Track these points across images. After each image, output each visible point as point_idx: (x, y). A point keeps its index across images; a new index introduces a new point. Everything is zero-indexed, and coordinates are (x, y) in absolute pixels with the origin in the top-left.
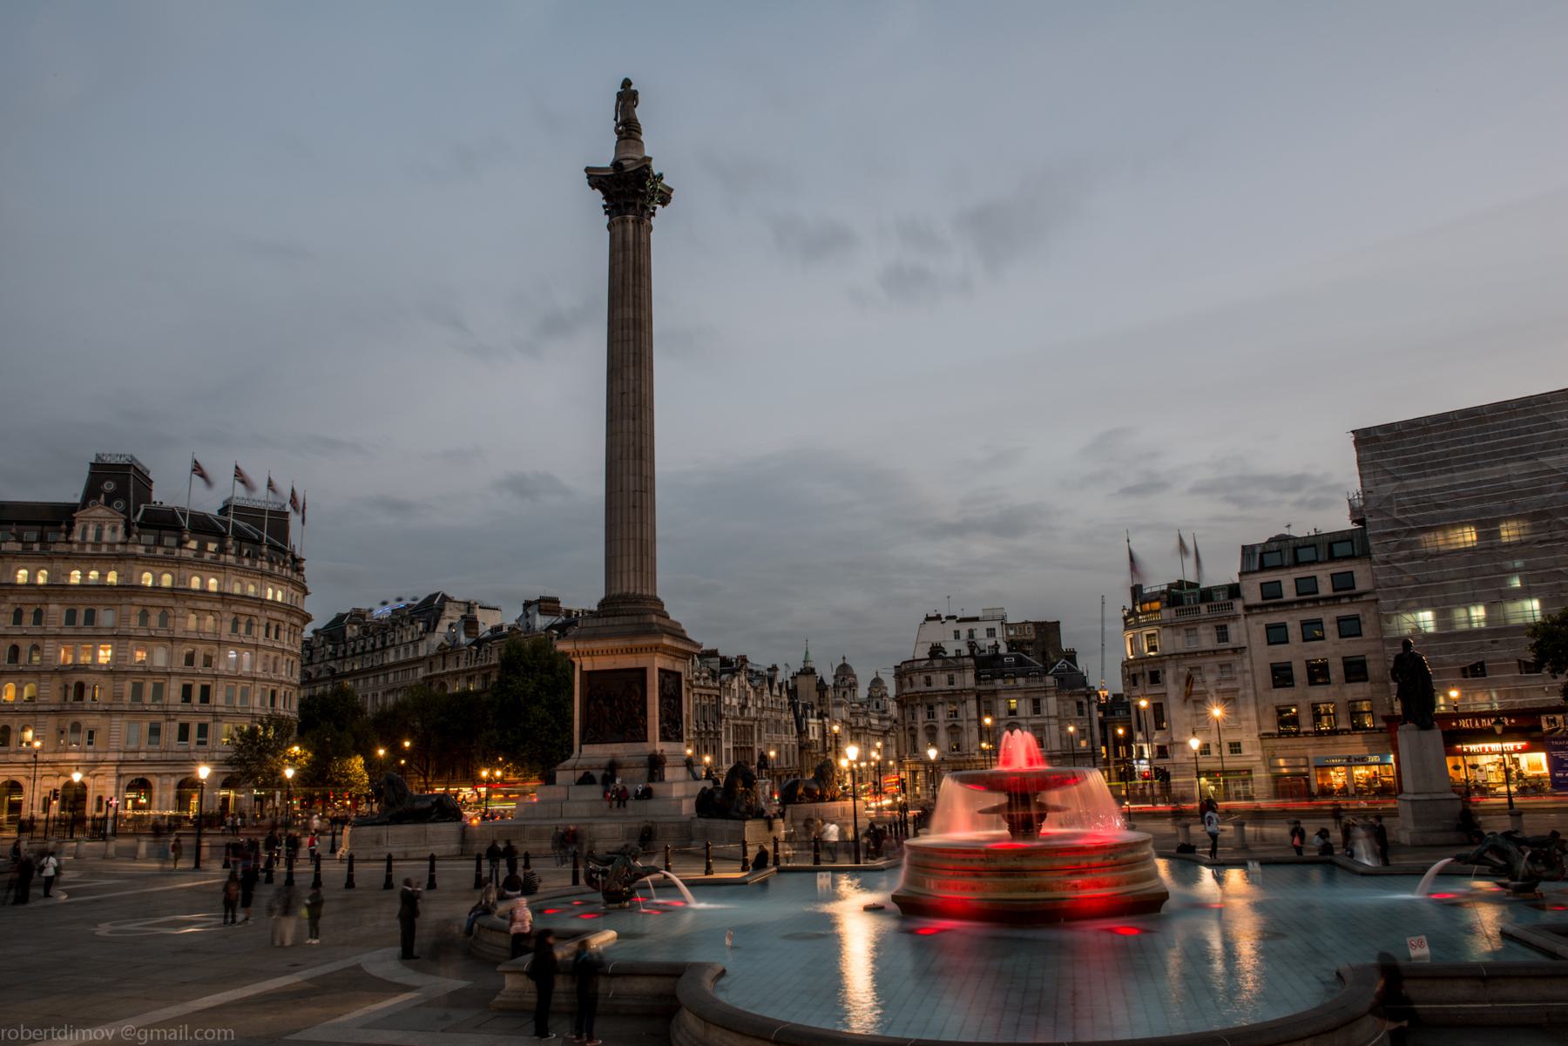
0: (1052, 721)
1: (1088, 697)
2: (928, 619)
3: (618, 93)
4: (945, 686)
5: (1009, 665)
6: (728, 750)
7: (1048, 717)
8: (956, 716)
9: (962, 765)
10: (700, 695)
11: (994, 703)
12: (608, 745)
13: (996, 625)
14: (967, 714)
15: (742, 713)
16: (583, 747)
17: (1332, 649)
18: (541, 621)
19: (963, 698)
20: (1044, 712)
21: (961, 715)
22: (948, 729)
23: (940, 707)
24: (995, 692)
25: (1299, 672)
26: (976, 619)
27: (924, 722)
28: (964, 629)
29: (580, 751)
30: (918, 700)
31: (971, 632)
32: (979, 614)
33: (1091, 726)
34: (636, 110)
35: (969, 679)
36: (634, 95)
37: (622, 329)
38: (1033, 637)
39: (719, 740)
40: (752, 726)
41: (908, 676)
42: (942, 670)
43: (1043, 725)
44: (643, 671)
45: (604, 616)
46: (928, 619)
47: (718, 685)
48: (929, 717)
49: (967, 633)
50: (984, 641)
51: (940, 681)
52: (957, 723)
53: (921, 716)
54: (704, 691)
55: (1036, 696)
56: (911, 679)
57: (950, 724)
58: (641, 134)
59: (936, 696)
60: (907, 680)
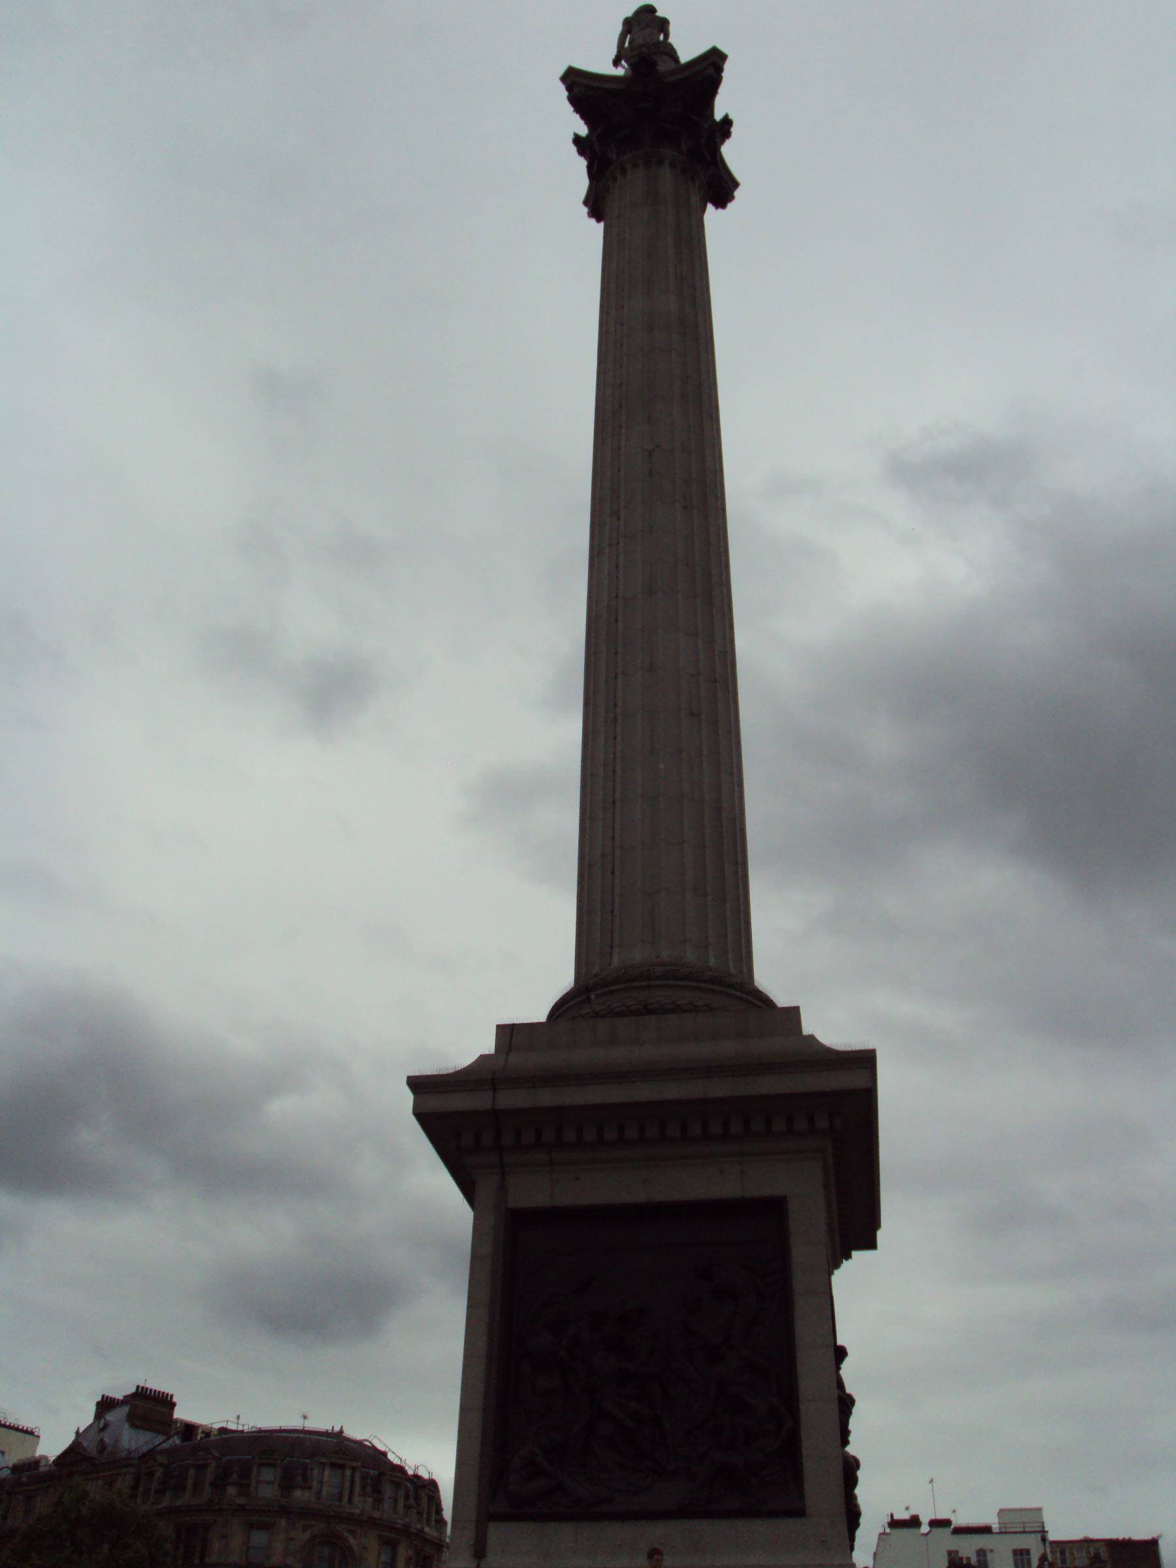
2: (894, 1524)
16: (496, 1532)
18: (132, 1440)
26: (986, 1530)
29: (479, 1552)
32: (993, 1521)
44: (775, 1208)
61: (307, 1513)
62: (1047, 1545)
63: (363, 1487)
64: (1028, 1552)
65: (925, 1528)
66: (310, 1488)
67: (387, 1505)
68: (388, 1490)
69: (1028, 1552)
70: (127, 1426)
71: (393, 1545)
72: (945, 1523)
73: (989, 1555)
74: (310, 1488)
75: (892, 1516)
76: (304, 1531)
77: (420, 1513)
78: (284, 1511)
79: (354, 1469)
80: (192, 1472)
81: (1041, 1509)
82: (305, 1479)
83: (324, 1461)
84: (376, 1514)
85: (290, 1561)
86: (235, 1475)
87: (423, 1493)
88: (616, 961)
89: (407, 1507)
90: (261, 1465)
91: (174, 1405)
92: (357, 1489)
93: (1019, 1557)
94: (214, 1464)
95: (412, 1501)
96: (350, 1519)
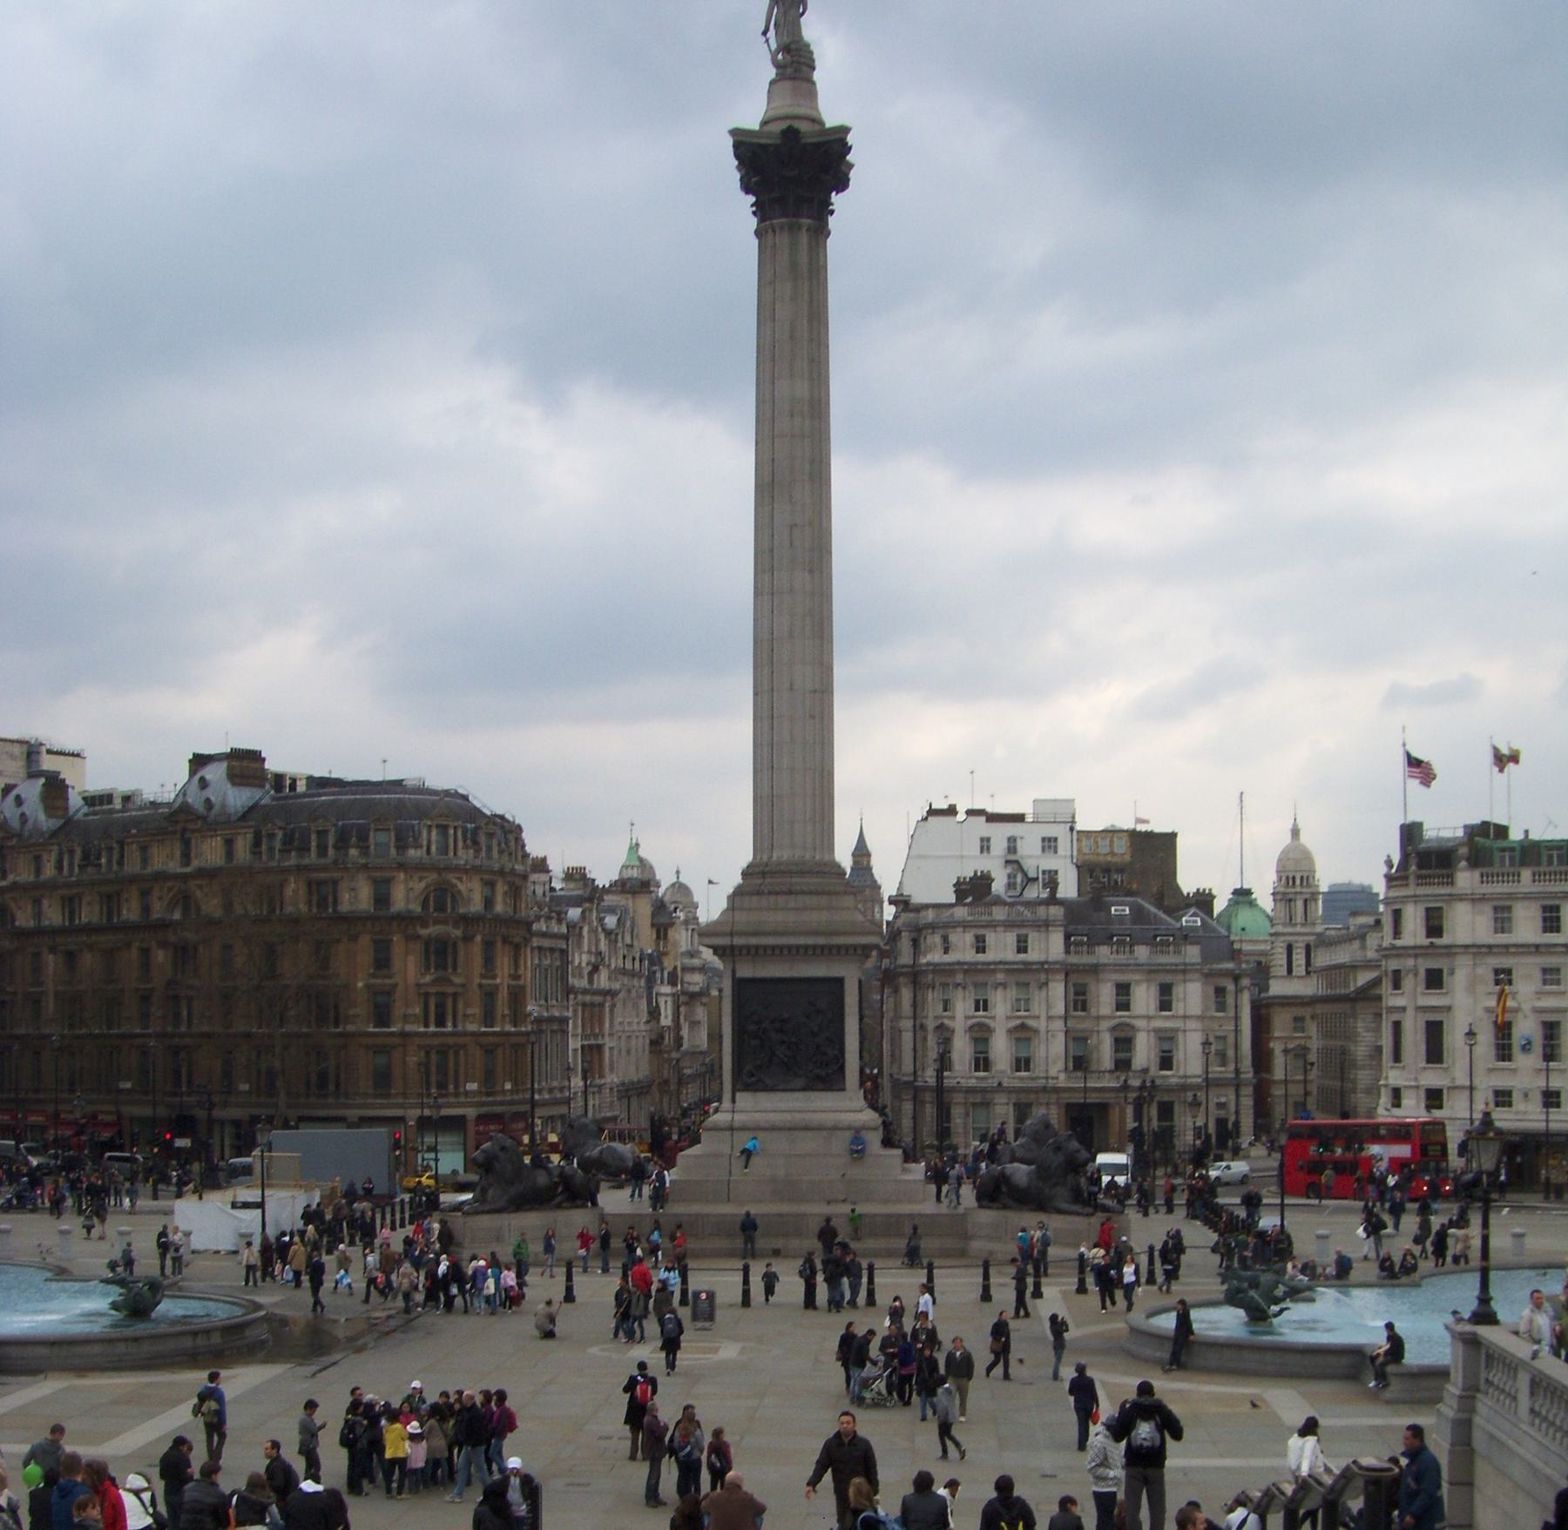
0: (1192, 1025)
1: (1236, 978)
2: (932, 812)
4: (1010, 955)
5: (1121, 918)
6: (575, 1050)
7: (1185, 1017)
9: (1032, 1096)
10: (540, 948)
11: (1092, 988)
12: (780, 1095)
13: (1060, 832)
14: (1049, 1007)
15: (591, 981)
16: (738, 1095)
18: (238, 798)
19: (1043, 977)
20: (1178, 1008)
21: (1038, 1008)
22: (1010, 1031)
23: (1000, 992)
24: (1095, 970)
26: (1019, 818)
27: (967, 1018)
28: (999, 833)
29: (734, 1101)
30: (959, 978)
32: (1026, 808)
33: (1237, 1031)
34: (803, 20)
35: (1049, 947)
37: (792, 416)
38: (1127, 858)
39: (565, 1032)
40: (602, 1005)
41: (941, 932)
42: (1009, 925)
43: (1177, 1030)
44: (840, 981)
45: (770, 893)
46: (932, 812)
47: (564, 929)
48: (977, 1009)
49: (1005, 844)
50: (1033, 858)
51: (1002, 947)
52: (1030, 1023)
53: (962, 1007)
54: (546, 943)
55: (1168, 979)
56: (945, 939)
57: (1018, 1022)
58: (813, 68)
59: (994, 971)
60: (937, 939)
61: (420, 868)
62: (1075, 833)
63: (465, 841)
64: (1056, 839)
65: (961, 816)
66: (421, 847)
67: (483, 854)
68: (483, 839)
69: (1056, 839)
70: (229, 786)
71: (491, 885)
73: (1019, 843)
74: (421, 847)
75: (931, 805)
76: (420, 881)
77: (510, 854)
78: (401, 866)
79: (455, 828)
80: (314, 837)
81: (1073, 800)
82: (416, 840)
83: (429, 823)
84: (478, 862)
85: (412, 907)
86: (354, 839)
87: (511, 837)
88: (775, 858)
89: (501, 852)
90: (377, 830)
91: (264, 760)
92: (460, 844)
93: (1046, 843)
94: (333, 829)
95: (503, 845)
96: (457, 869)
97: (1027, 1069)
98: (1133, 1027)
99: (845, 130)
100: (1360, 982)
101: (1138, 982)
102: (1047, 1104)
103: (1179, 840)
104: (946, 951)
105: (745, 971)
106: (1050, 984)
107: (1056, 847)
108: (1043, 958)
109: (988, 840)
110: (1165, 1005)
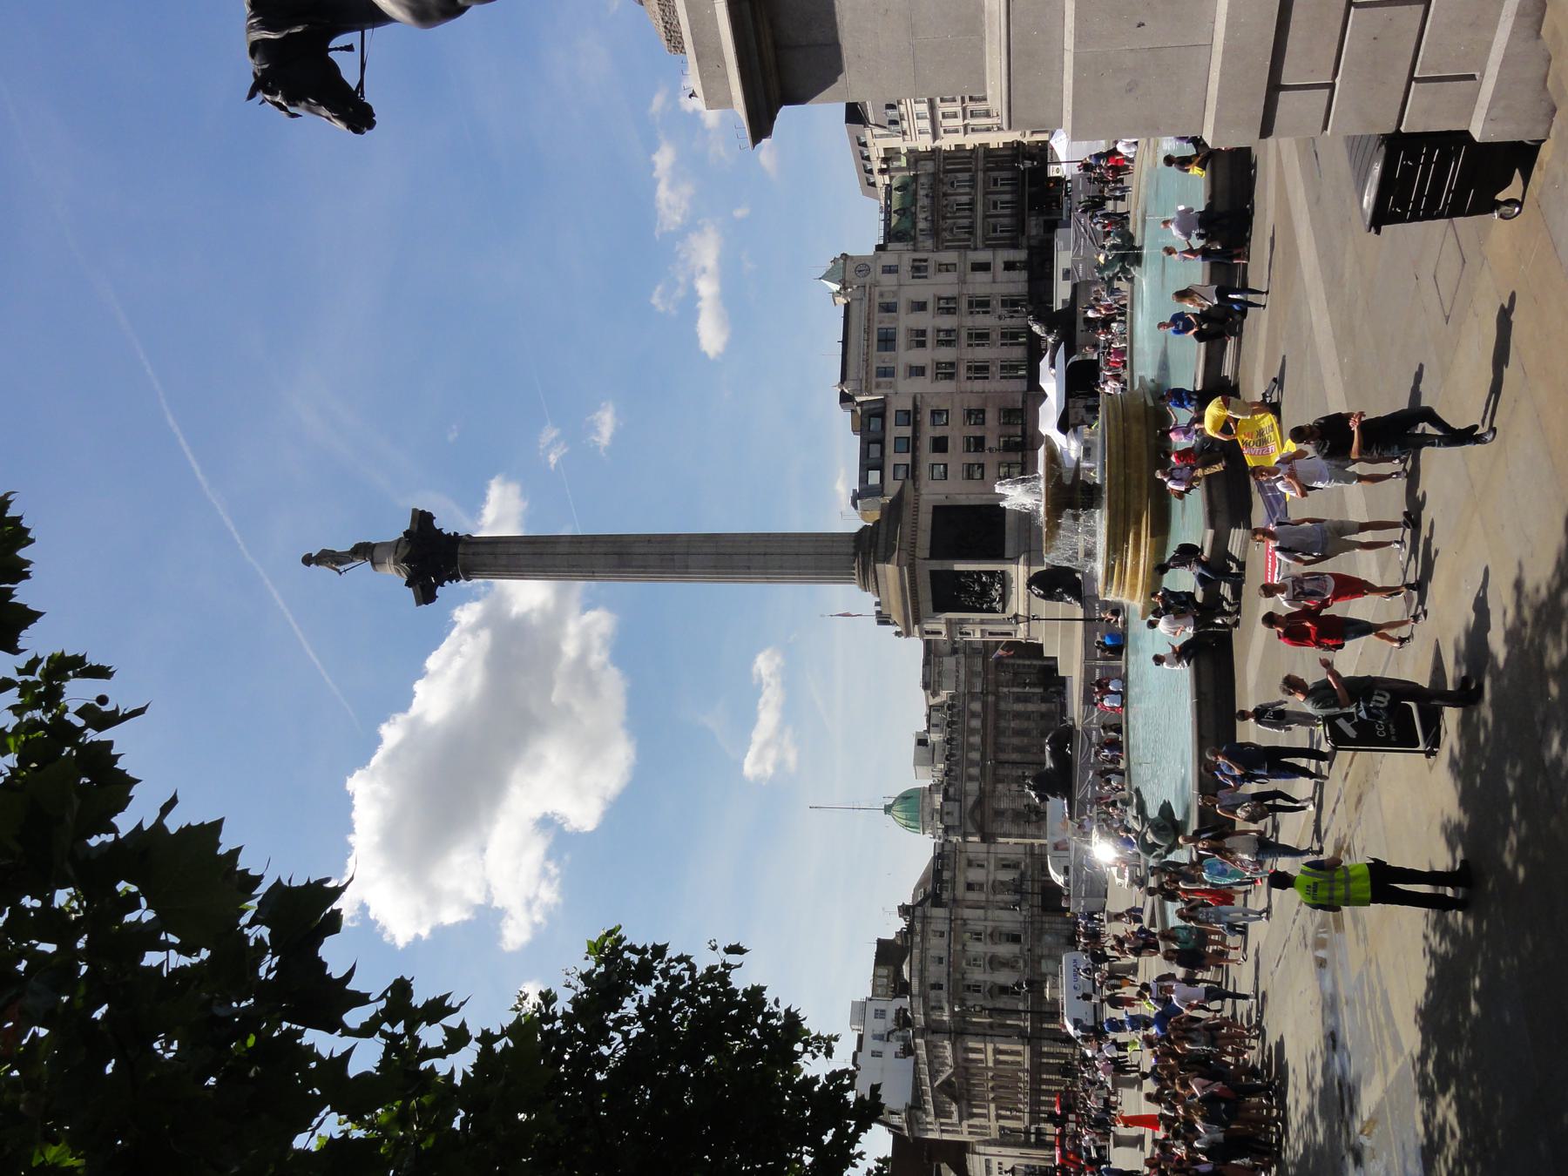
3: (317, 564)
4: (944, 941)
8: (980, 934)
14: (979, 919)
17: (956, 432)
21: (979, 927)
25: (972, 458)
26: (860, 1038)
28: (870, 1045)
31: (879, 1037)
32: (856, 1034)
36: (324, 551)
38: (892, 968)
52: (989, 931)
53: (977, 975)
55: (964, 863)
60: (933, 994)
64: (876, 1010)
69: (876, 1010)
72: (855, 1055)
73: (877, 1032)
97: (1020, 936)
98: (994, 882)
99: (415, 510)
100: (973, 831)
101: (966, 877)
102: (1042, 922)
103: (883, 937)
104: (940, 987)
105: (926, 554)
106: (965, 917)
107: (883, 1011)
108: (947, 921)
109: (873, 1052)
110: (982, 866)
